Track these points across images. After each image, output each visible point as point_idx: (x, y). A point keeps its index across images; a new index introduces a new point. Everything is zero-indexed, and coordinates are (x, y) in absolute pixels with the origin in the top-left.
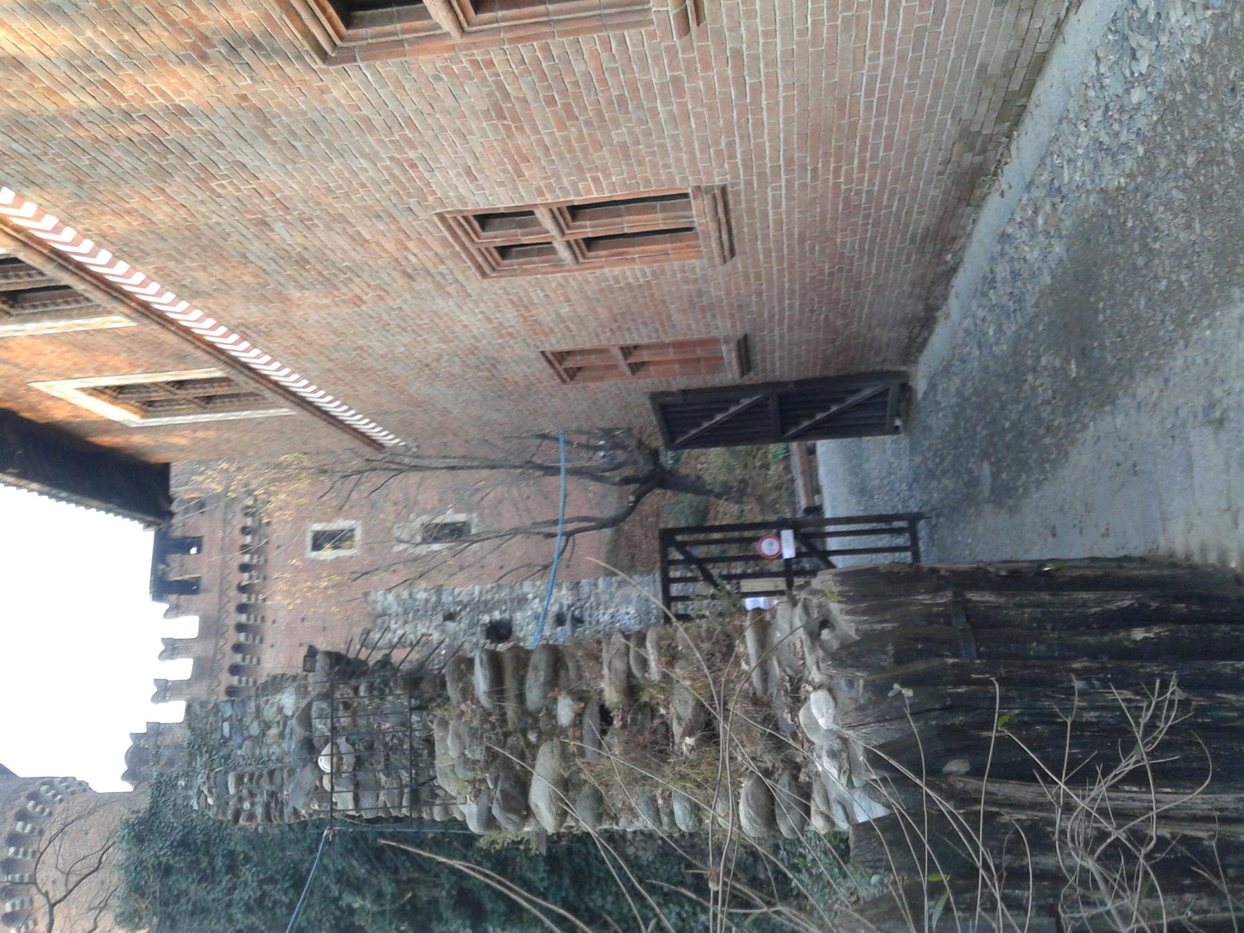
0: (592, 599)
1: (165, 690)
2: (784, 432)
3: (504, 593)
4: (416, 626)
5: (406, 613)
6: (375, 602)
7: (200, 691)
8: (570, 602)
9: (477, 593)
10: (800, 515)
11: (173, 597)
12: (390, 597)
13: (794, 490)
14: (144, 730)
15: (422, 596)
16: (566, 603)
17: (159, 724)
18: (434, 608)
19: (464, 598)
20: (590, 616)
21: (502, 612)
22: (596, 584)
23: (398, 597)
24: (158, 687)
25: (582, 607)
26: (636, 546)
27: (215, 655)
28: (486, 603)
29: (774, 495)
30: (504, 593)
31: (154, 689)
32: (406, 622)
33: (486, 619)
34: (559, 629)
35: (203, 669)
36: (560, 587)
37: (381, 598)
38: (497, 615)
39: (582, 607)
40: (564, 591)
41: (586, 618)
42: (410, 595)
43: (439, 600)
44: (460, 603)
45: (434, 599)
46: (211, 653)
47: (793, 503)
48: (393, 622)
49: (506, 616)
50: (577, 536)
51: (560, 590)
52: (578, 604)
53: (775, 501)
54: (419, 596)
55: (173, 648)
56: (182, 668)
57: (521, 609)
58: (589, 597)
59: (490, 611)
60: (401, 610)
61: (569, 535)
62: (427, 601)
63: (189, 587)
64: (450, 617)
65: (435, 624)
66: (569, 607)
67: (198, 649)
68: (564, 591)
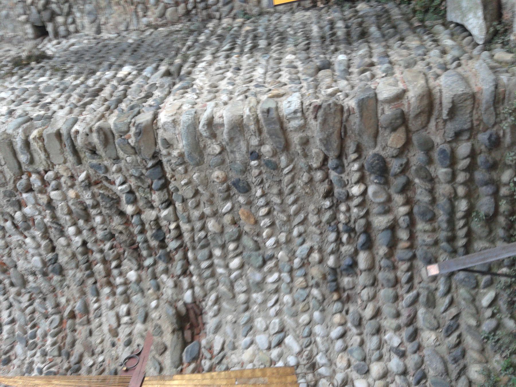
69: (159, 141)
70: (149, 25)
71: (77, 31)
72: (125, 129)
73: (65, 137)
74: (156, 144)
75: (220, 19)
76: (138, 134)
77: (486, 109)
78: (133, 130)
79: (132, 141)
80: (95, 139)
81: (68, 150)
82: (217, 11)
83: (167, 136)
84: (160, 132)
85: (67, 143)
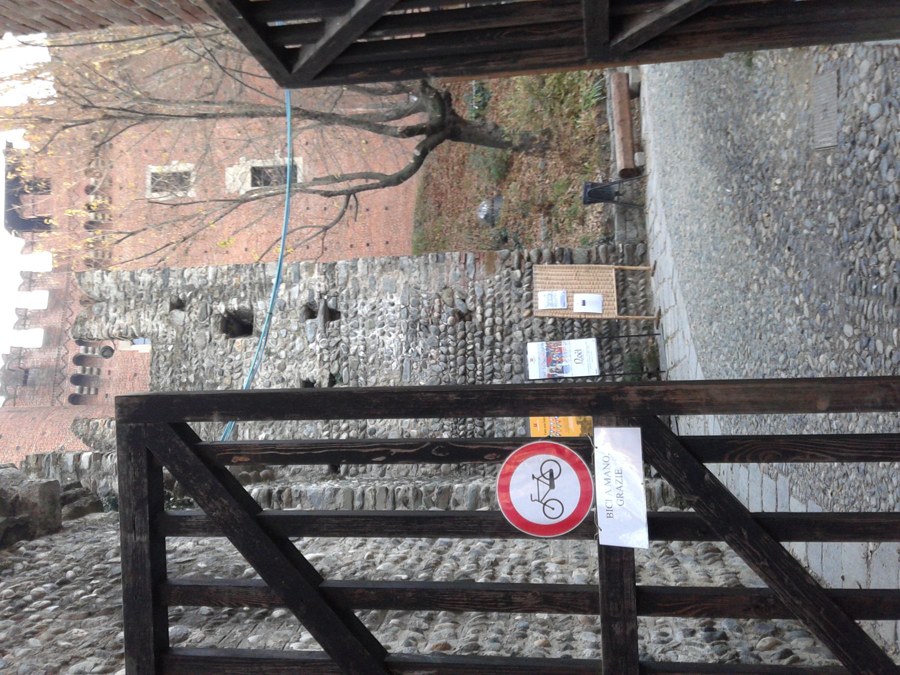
0: (350, 285)
1: (25, 319)
2: (617, 24)
3: (244, 277)
4: (138, 316)
5: (127, 298)
6: (91, 285)
7: (55, 320)
8: (322, 289)
9: (210, 277)
10: (614, 177)
11: (28, 235)
12: (109, 279)
13: (608, 145)
14: (8, 352)
15: (145, 278)
16: (316, 289)
17: (21, 349)
18: (160, 293)
19: (196, 282)
20: (347, 307)
21: (240, 300)
22: (354, 268)
23: (118, 277)
24: (19, 316)
25: (336, 296)
26: (442, 194)
27: (67, 287)
28: (222, 288)
29: (584, 151)
30: (244, 277)
31: (16, 319)
32: (126, 310)
33: (221, 308)
34: (309, 321)
35: (58, 300)
36: (310, 269)
37: (97, 280)
38: (234, 304)
39: (336, 296)
40: (316, 275)
41: (342, 309)
42: (132, 277)
43: (165, 284)
44: (191, 287)
45: (160, 282)
46: (64, 286)
47: (606, 163)
48: (111, 310)
49: (246, 305)
50: (357, 194)
51: (311, 273)
52: (332, 291)
53: (584, 160)
54: (141, 279)
55: (30, 281)
56: (39, 299)
57: (263, 297)
58: (346, 284)
59: (225, 299)
60: (120, 295)
61: (349, 193)
62: (152, 284)
63: (39, 224)
64: (179, 305)
65: (161, 312)
66: (321, 296)
67: (53, 282)
68: (316, 275)
69: (451, 501)
70: (425, 474)
71: (365, 472)
72: (431, 489)
73: (390, 492)
74: (449, 503)
75: (484, 475)
76: (439, 493)
77: (659, 499)
78: (436, 491)
79: (434, 498)
80: (410, 494)
81: (390, 500)
82: (483, 469)
83: (458, 497)
84: (453, 495)
85: (391, 496)
